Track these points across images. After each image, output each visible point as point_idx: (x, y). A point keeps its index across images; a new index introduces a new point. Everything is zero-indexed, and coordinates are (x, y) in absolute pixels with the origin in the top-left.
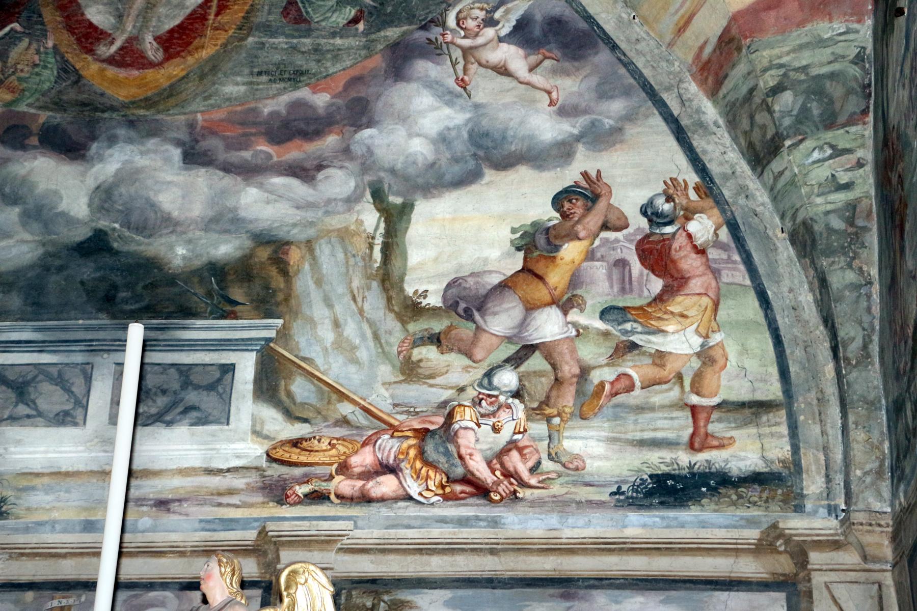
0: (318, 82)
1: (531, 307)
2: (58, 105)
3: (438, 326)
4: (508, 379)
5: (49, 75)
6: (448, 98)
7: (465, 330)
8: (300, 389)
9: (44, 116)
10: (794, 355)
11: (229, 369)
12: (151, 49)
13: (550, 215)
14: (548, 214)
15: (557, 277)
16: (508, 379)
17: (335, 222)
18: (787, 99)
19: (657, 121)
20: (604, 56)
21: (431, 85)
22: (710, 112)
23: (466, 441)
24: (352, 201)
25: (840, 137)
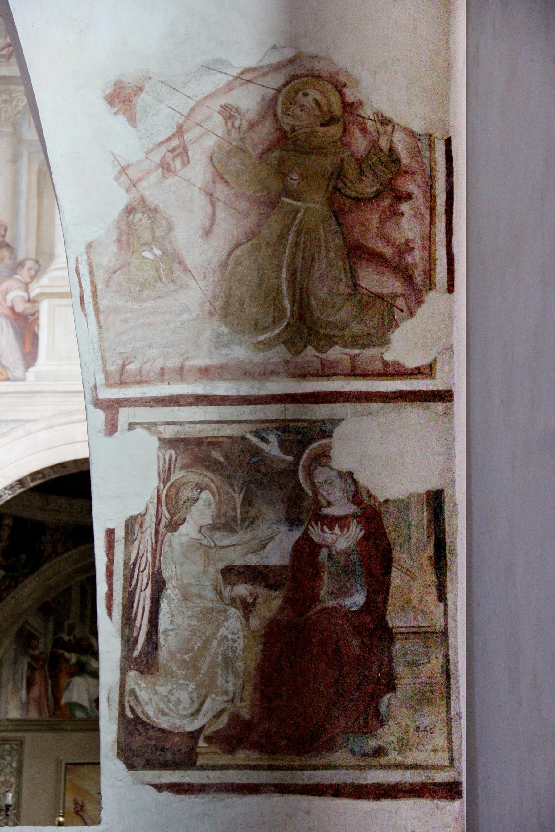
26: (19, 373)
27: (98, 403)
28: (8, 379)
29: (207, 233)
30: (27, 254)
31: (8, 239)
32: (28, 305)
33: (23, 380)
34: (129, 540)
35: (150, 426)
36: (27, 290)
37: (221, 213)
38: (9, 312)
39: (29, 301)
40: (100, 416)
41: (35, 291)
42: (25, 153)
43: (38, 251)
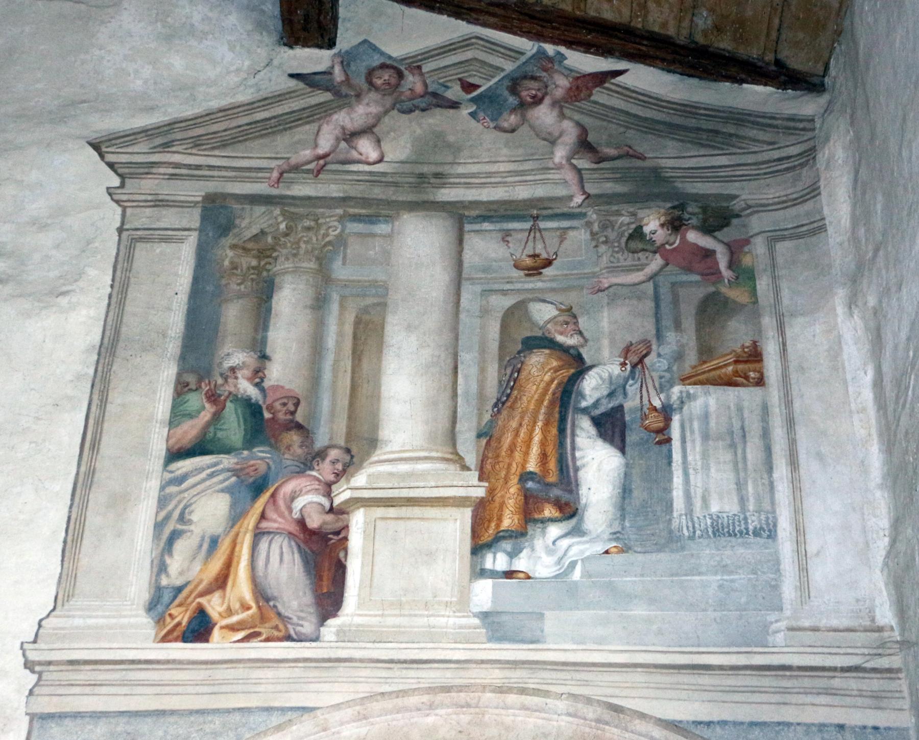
26: (308, 628)
28: (289, 638)
30: (331, 439)
31: (299, 417)
32: (330, 518)
33: (316, 639)
36: (328, 494)
38: (293, 528)
39: (331, 510)
41: (342, 495)
42: (335, 297)
43: (349, 436)
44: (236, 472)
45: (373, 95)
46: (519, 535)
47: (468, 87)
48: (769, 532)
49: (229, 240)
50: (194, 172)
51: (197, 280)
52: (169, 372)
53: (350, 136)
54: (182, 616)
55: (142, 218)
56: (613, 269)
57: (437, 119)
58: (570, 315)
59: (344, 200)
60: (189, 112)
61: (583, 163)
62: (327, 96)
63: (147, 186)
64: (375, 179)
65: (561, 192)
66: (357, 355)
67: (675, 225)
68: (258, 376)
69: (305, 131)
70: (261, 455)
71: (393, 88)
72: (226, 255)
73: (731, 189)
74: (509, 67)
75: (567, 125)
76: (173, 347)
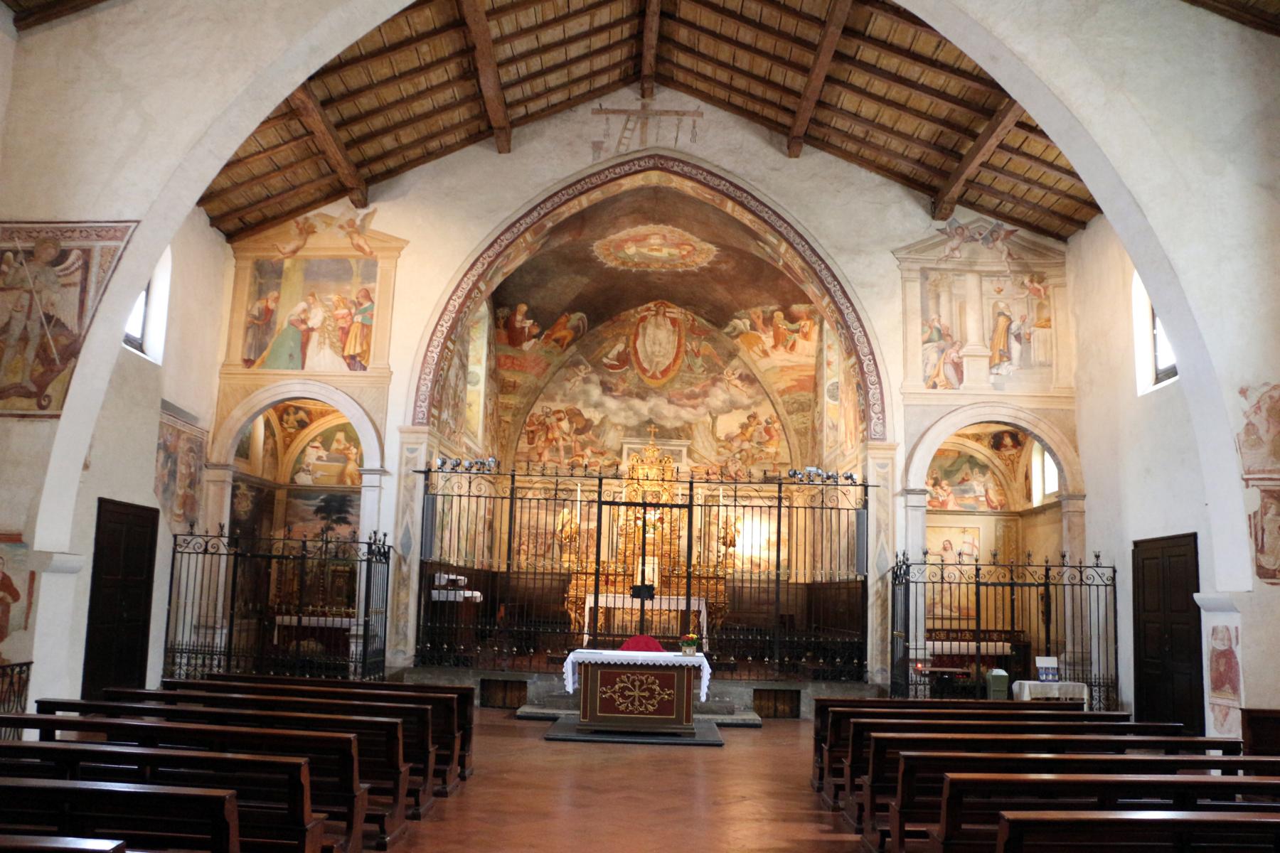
0: (696, 385)
1: (743, 441)
2: (639, 388)
3: (724, 444)
4: (738, 456)
5: (636, 380)
6: (724, 391)
7: (729, 445)
8: (696, 456)
9: (636, 390)
10: (793, 454)
11: (681, 451)
12: (659, 375)
13: (746, 421)
14: (746, 421)
15: (748, 435)
16: (738, 456)
17: (701, 419)
18: (795, 405)
19: (768, 402)
20: (757, 385)
21: (721, 388)
22: (779, 400)
23: (730, 469)
24: (705, 414)
25: (805, 414)
27: (1243, 479)
29: (1268, 431)
34: (1255, 517)
35: (1257, 486)
37: (1271, 427)
40: (1244, 483)
41: (961, 354)
44: (938, 347)
45: (957, 237)
46: (999, 364)
47: (980, 234)
48: (1050, 365)
49: (928, 282)
50: (916, 261)
51: (922, 294)
52: (919, 321)
53: (953, 250)
54: (931, 383)
55: (906, 274)
56: (1018, 294)
57: (973, 245)
58: (1008, 306)
59: (953, 270)
60: (913, 242)
61: (1009, 260)
62: (946, 237)
63: (906, 265)
64: (960, 263)
65: (1003, 269)
66: (960, 315)
67: (1032, 281)
68: (939, 321)
69: (941, 248)
70: (942, 343)
71: (962, 234)
72: (928, 287)
73: (1045, 270)
74: (990, 228)
75: (1005, 248)
76: (919, 313)
